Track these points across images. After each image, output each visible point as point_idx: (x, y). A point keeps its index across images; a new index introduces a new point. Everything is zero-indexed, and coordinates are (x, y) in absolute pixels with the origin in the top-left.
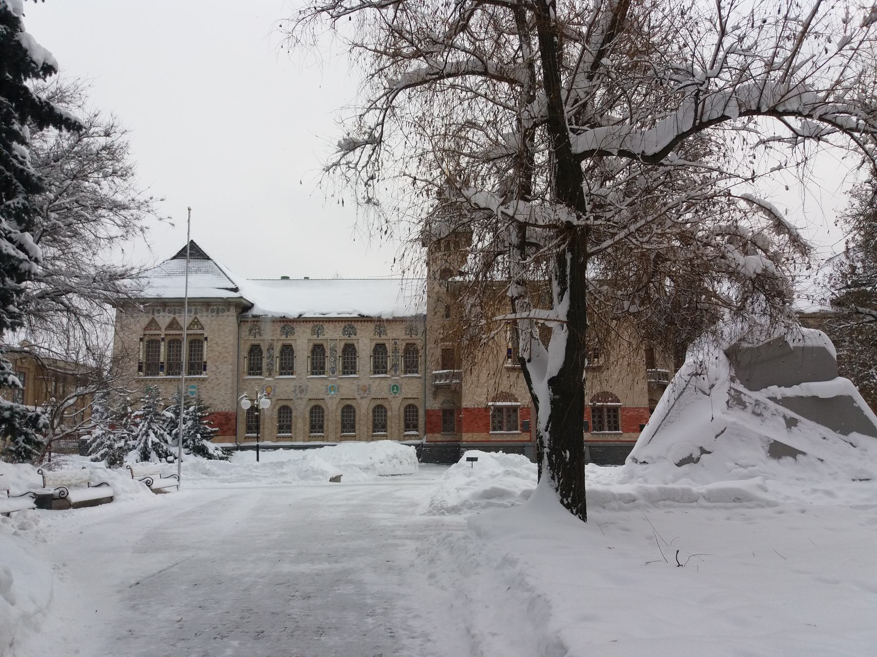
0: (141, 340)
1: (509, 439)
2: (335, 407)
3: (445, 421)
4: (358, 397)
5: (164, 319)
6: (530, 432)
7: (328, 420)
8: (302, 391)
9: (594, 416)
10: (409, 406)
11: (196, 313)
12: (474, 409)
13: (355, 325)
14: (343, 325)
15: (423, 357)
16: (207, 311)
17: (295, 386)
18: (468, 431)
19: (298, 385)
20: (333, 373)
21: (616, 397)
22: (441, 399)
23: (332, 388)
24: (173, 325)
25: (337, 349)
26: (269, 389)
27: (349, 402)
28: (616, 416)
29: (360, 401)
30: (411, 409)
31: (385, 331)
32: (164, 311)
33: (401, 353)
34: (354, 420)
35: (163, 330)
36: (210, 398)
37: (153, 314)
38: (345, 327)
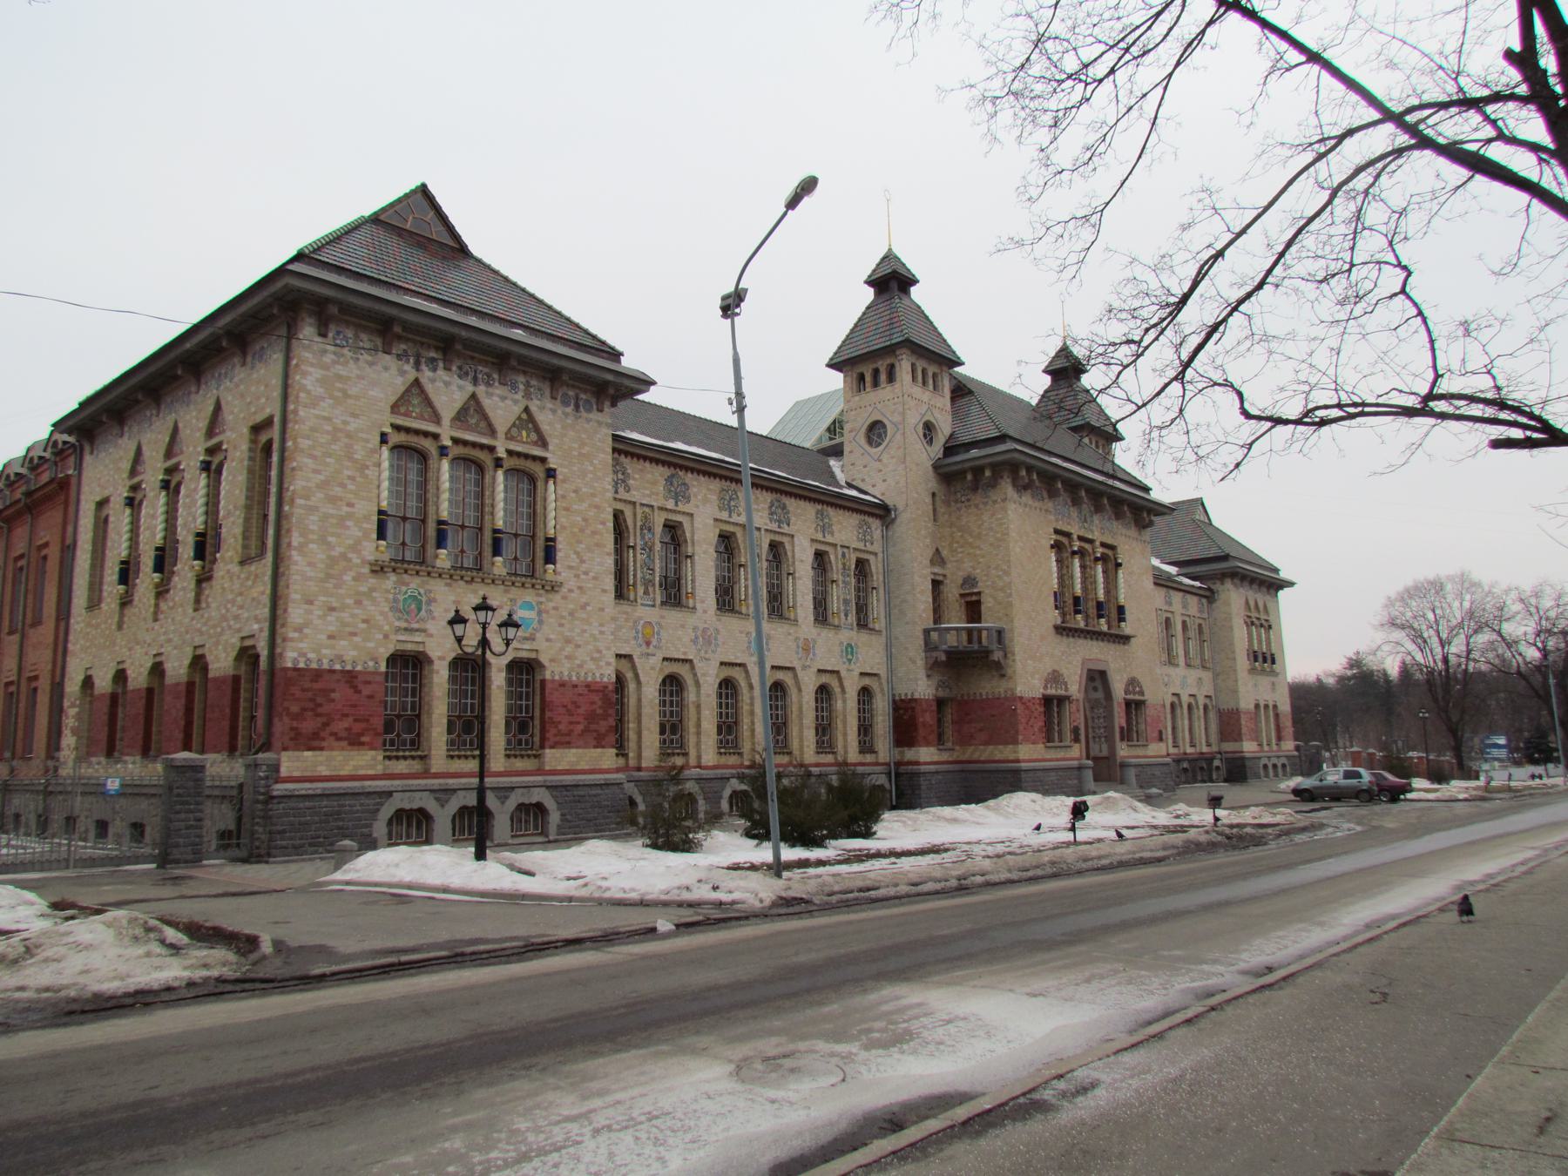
0: (384, 439)
4: (796, 664)
5: (448, 390)
11: (527, 396)
13: (791, 503)
15: (881, 591)
16: (553, 398)
17: (695, 629)
19: (701, 626)
22: (937, 678)
24: (472, 411)
26: (648, 630)
27: (780, 675)
29: (800, 673)
32: (447, 369)
35: (446, 421)
36: (568, 641)
37: (417, 366)
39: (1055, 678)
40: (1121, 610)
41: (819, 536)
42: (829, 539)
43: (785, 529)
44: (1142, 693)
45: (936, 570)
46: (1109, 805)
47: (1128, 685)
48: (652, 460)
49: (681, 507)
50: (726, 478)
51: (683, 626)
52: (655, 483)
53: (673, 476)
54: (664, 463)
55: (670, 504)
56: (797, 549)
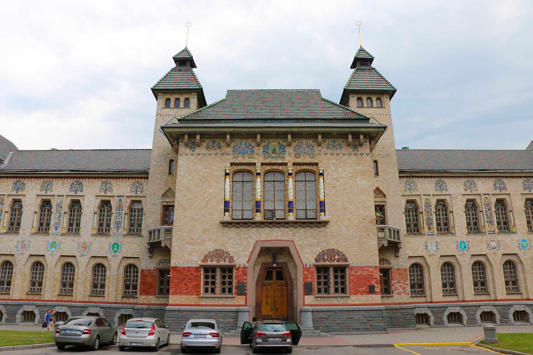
1: (221, 302)
2: (54, 264)
3: (162, 283)
4: (76, 254)
6: (245, 294)
7: (46, 276)
8: (24, 247)
9: (319, 277)
10: (130, 266)
12: (184, 269)
13: (85, 182)
14: (71, 181)
17: (18, 242)
18: (175, 293)
20: (56, 229)
21: (343, 255)
22: (158, 258)
23: (53, 244)
25: (63, 205)
28: (343, 277)
29: (78, 258)
30: (132, 270)
31: (111, 188)
33: (126, 210)
34: (73, 278)
38: (73, 184)
39: (219, 254)
40: (322, 204)
41: (103, 194)
42: (108, 194)
43: (79, 193)
44: (346, 260)
45: (167, 200)
46: (176, 336)
47: (323, 253)
48: (7, 177)
49: (19, 193)
50: (47, 177)
51: (11, 241)
52: (8, 186)
53: (18, 181)
54: (13, 177)
55: (14, 193)
56: (86, 201)
